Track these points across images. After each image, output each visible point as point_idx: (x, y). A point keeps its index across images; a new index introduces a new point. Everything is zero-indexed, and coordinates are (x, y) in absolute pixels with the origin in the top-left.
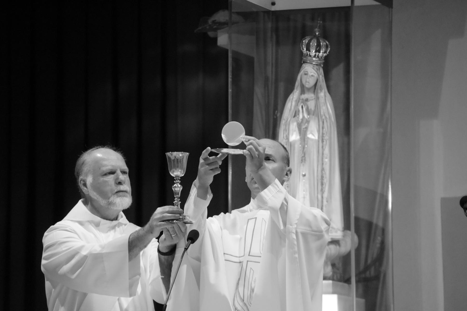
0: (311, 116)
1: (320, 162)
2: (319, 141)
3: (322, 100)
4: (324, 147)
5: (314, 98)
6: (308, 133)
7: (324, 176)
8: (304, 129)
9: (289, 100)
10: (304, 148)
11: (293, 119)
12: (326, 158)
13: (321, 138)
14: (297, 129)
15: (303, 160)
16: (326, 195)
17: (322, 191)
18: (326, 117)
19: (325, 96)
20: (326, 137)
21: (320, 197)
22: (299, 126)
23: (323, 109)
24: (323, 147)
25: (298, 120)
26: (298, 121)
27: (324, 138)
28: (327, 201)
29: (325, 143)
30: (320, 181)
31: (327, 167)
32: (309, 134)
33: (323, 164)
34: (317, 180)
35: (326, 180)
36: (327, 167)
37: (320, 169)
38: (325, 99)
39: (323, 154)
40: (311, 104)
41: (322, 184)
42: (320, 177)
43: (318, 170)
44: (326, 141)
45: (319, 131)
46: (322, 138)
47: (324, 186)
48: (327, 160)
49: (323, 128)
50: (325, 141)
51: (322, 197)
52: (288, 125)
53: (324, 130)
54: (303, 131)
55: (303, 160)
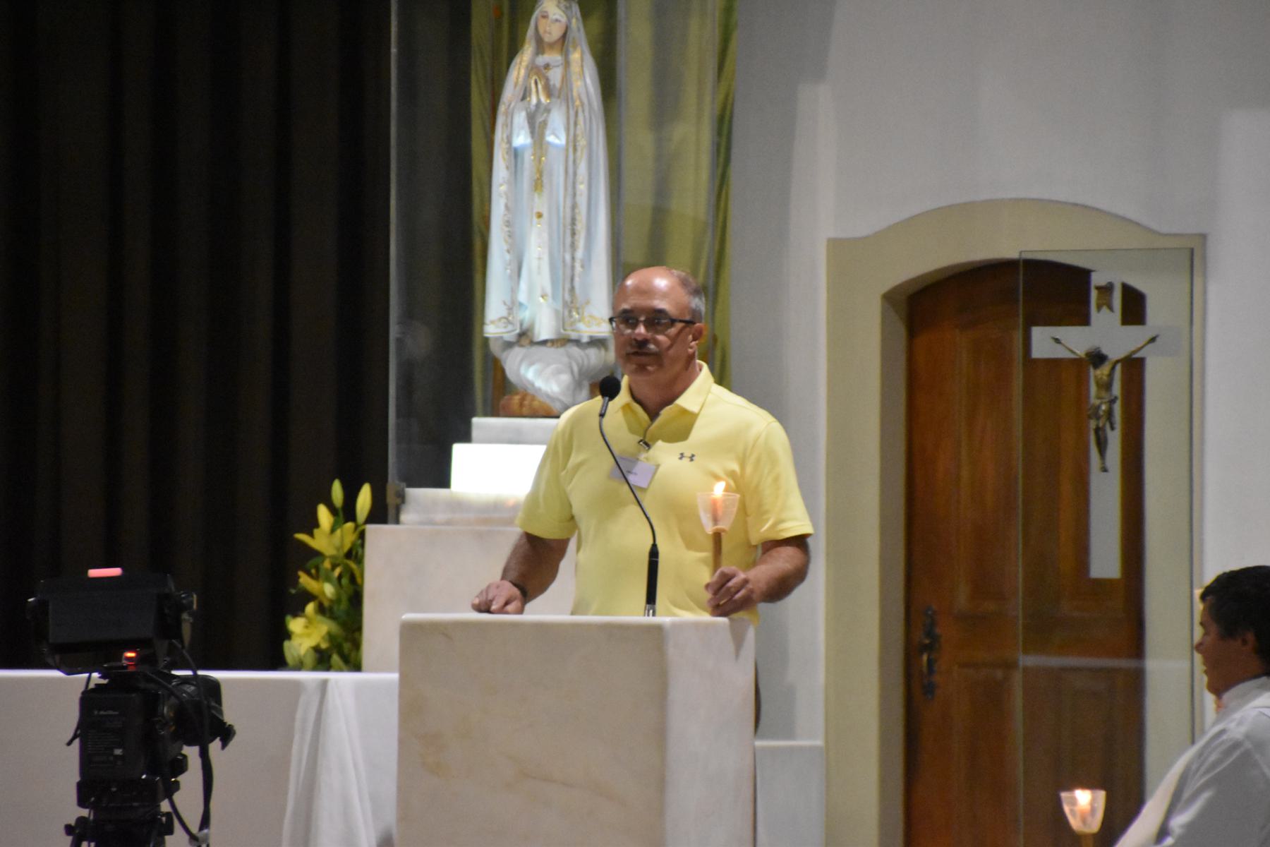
0: (554, 100)
1: (570, 189)
2: (567, 150)
3: (575, 68)
4: (578, 161)
5: (560, 62)
6: (547, 132)
7: (578, 217)
8: (540, 123)
9: (514, 66)
10: (540, 161)
11: (521, 104)
12: (582, 183)
13: (571, 144)
14: (526, 125)
15: (538, 185)
16: (579, 254)
17: (573, 246)
18: (582, 104)
19: (582, 60)
20: (582, 142)
21: (568, 257)
22: (531, 119)
23: (577, 85)
24: (574, 161)
25: (529, 108)
26: (529, 110)
27: (578, 144)
28: (582, 266)
29: (579, 153)
30: (569, 227)
31: (582, 201)
32: (549, 135)
33: (574, 195)
34: (564, 226)
35: (581, 227)
36: (582, 201)
37: (569, 204)
38: (582, 66)
39: (575, 174)
40: (555, 76)
41: (573, 234)
42: (568, 220)
43: (564, 207)
44: (582, 150)
45: (568, 130)
46: (573, 143)
47: (577, 237)
48: (582, 187)
49: (576, 124)
50: (579, 149)
51: (573, 258)
52: (510, 115)
53: (578, 127)
54: (539, 127)
55: (538, 185)
